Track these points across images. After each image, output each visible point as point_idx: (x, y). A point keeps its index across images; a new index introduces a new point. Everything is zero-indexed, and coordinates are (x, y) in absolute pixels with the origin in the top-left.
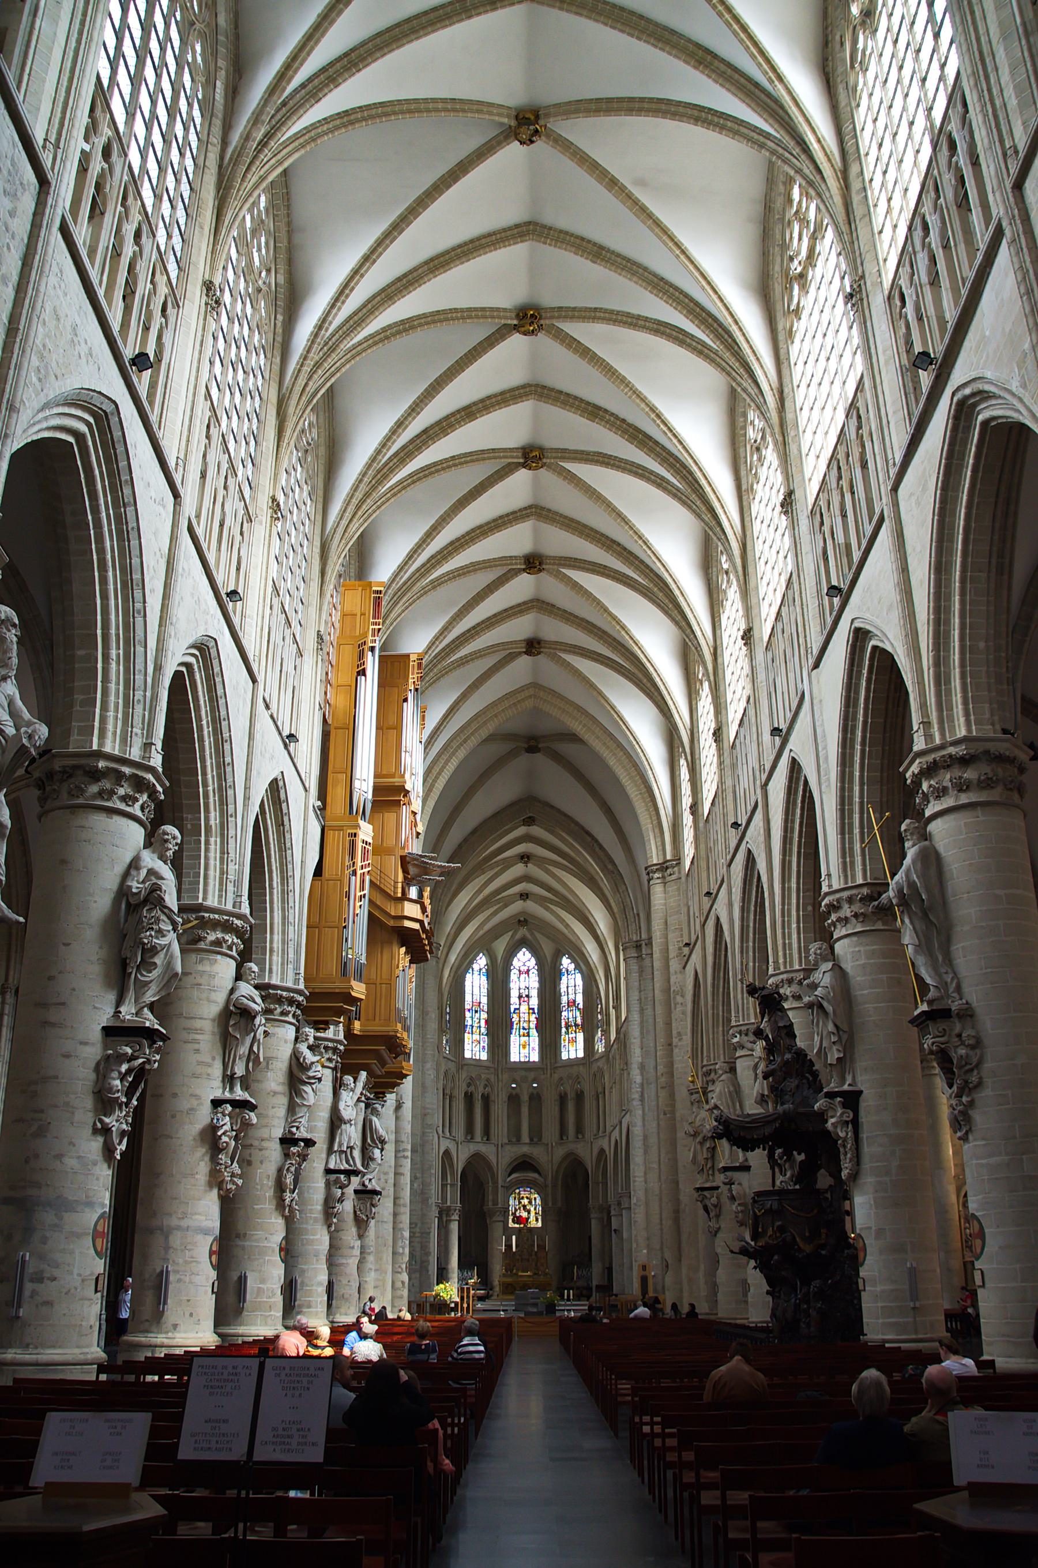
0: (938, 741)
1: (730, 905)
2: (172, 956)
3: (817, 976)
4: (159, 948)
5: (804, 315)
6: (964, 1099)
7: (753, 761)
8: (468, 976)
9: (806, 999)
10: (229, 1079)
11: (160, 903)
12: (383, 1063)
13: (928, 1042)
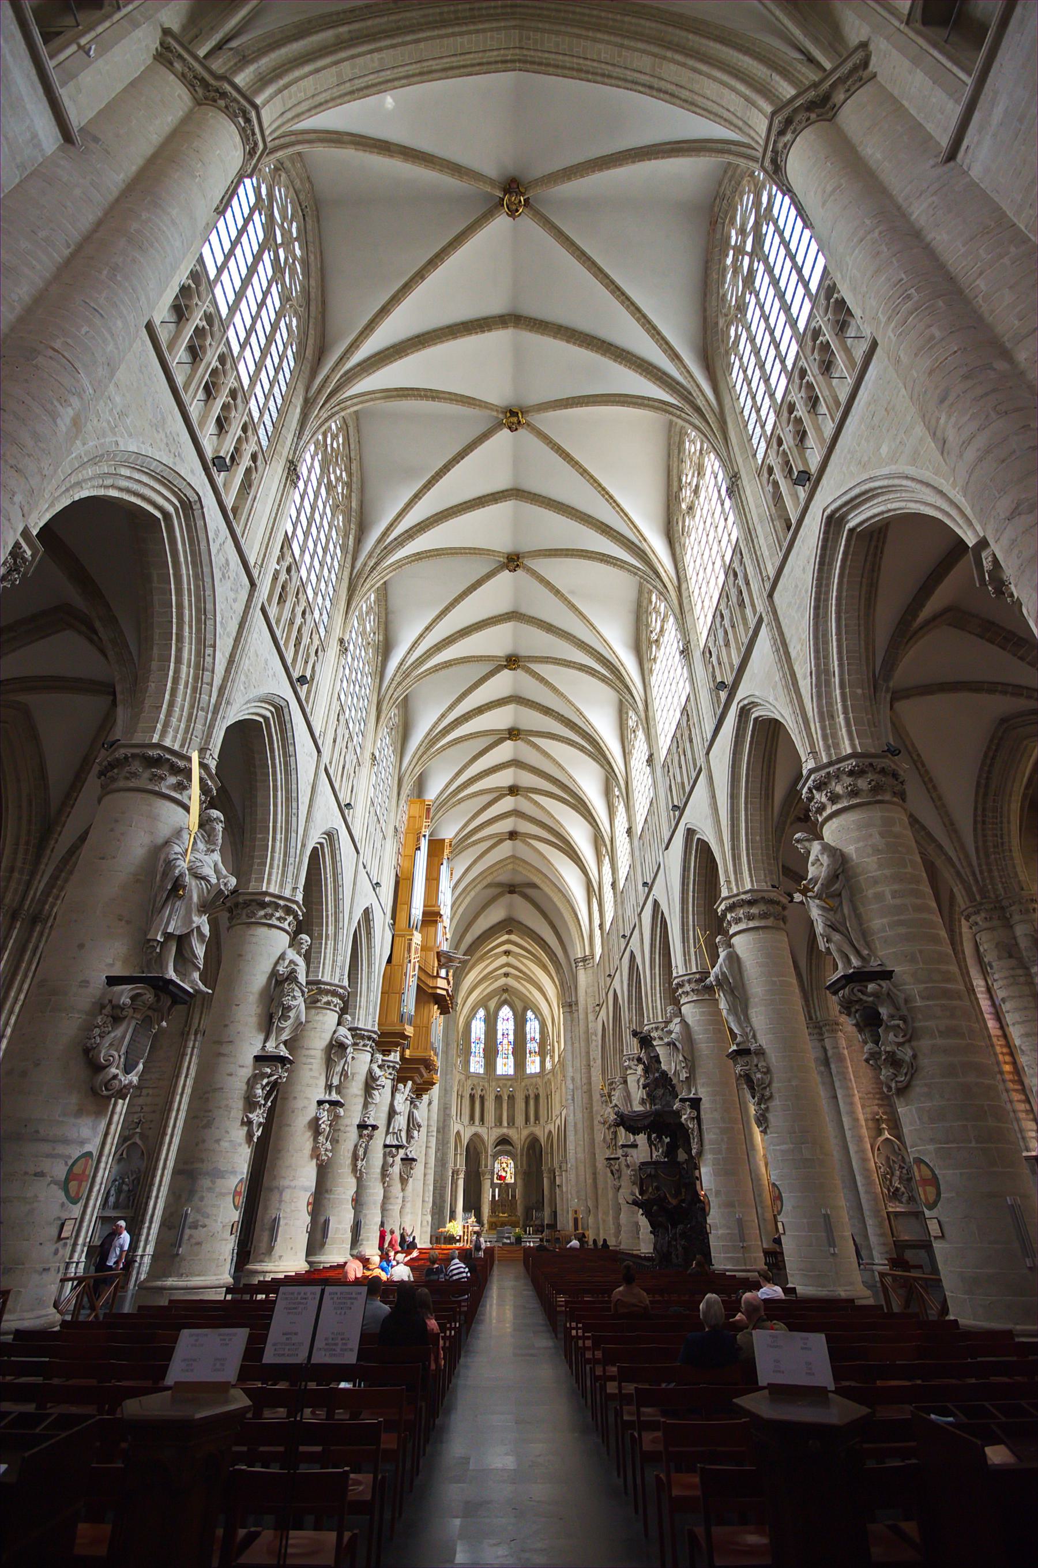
0: (735, 891)
1: (622, 982)
3: (671, 1026)
5: (658, 661)
6: (763, 1106)
7: (633, 901)
8: (474, 1023)
9: (666, 1040)
10: (329, 1087)
11: (295, 980)
12: (422, 1076)
13: (738, 1069)
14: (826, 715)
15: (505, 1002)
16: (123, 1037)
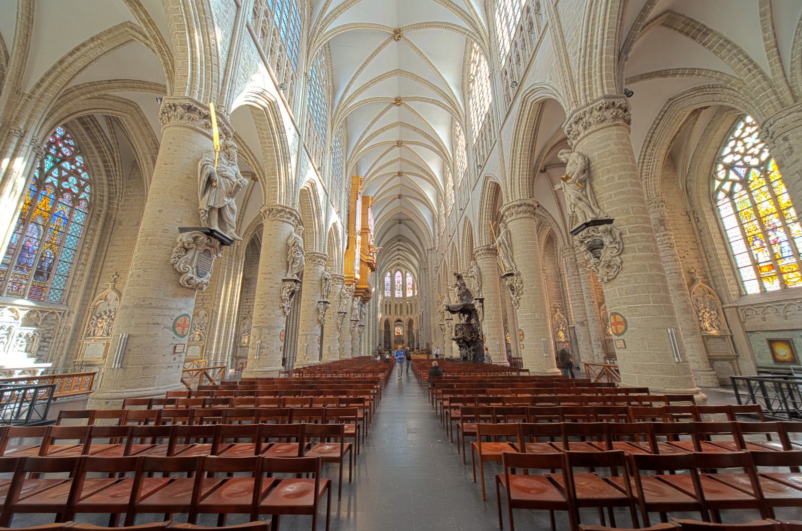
7: (455, 220)
14: (587, 76)
15: (398, 270)
16: (193, 259)
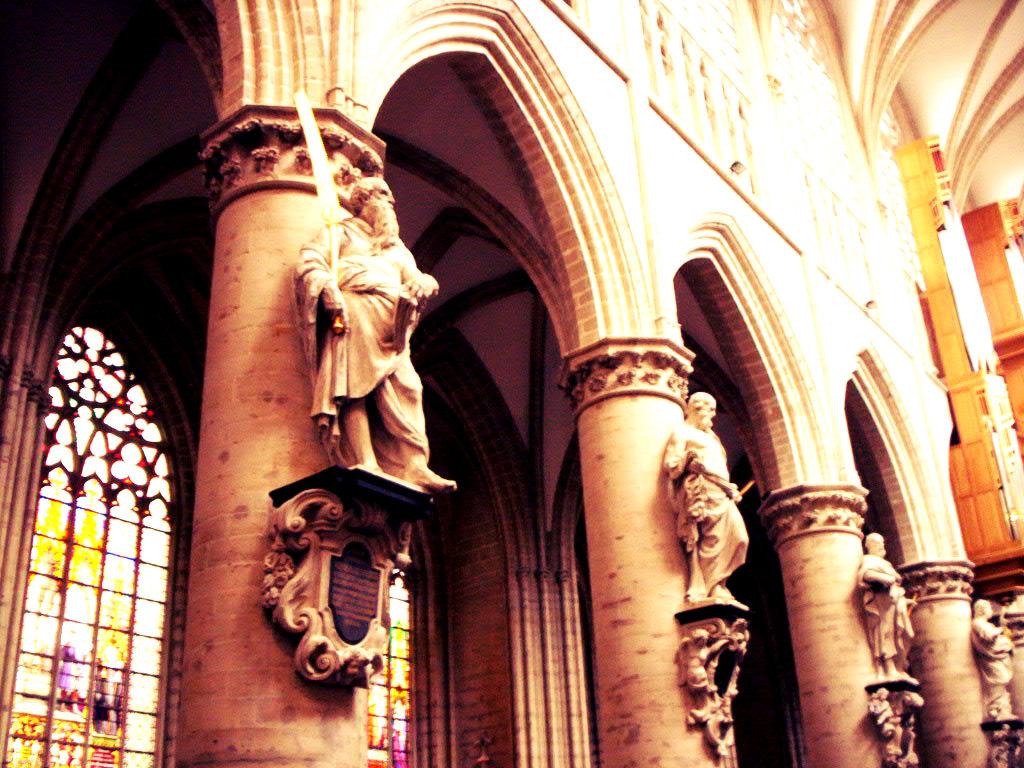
2: (733, 526)
4: (714, 519)
10: (880, 661)
16: (317, 581)
